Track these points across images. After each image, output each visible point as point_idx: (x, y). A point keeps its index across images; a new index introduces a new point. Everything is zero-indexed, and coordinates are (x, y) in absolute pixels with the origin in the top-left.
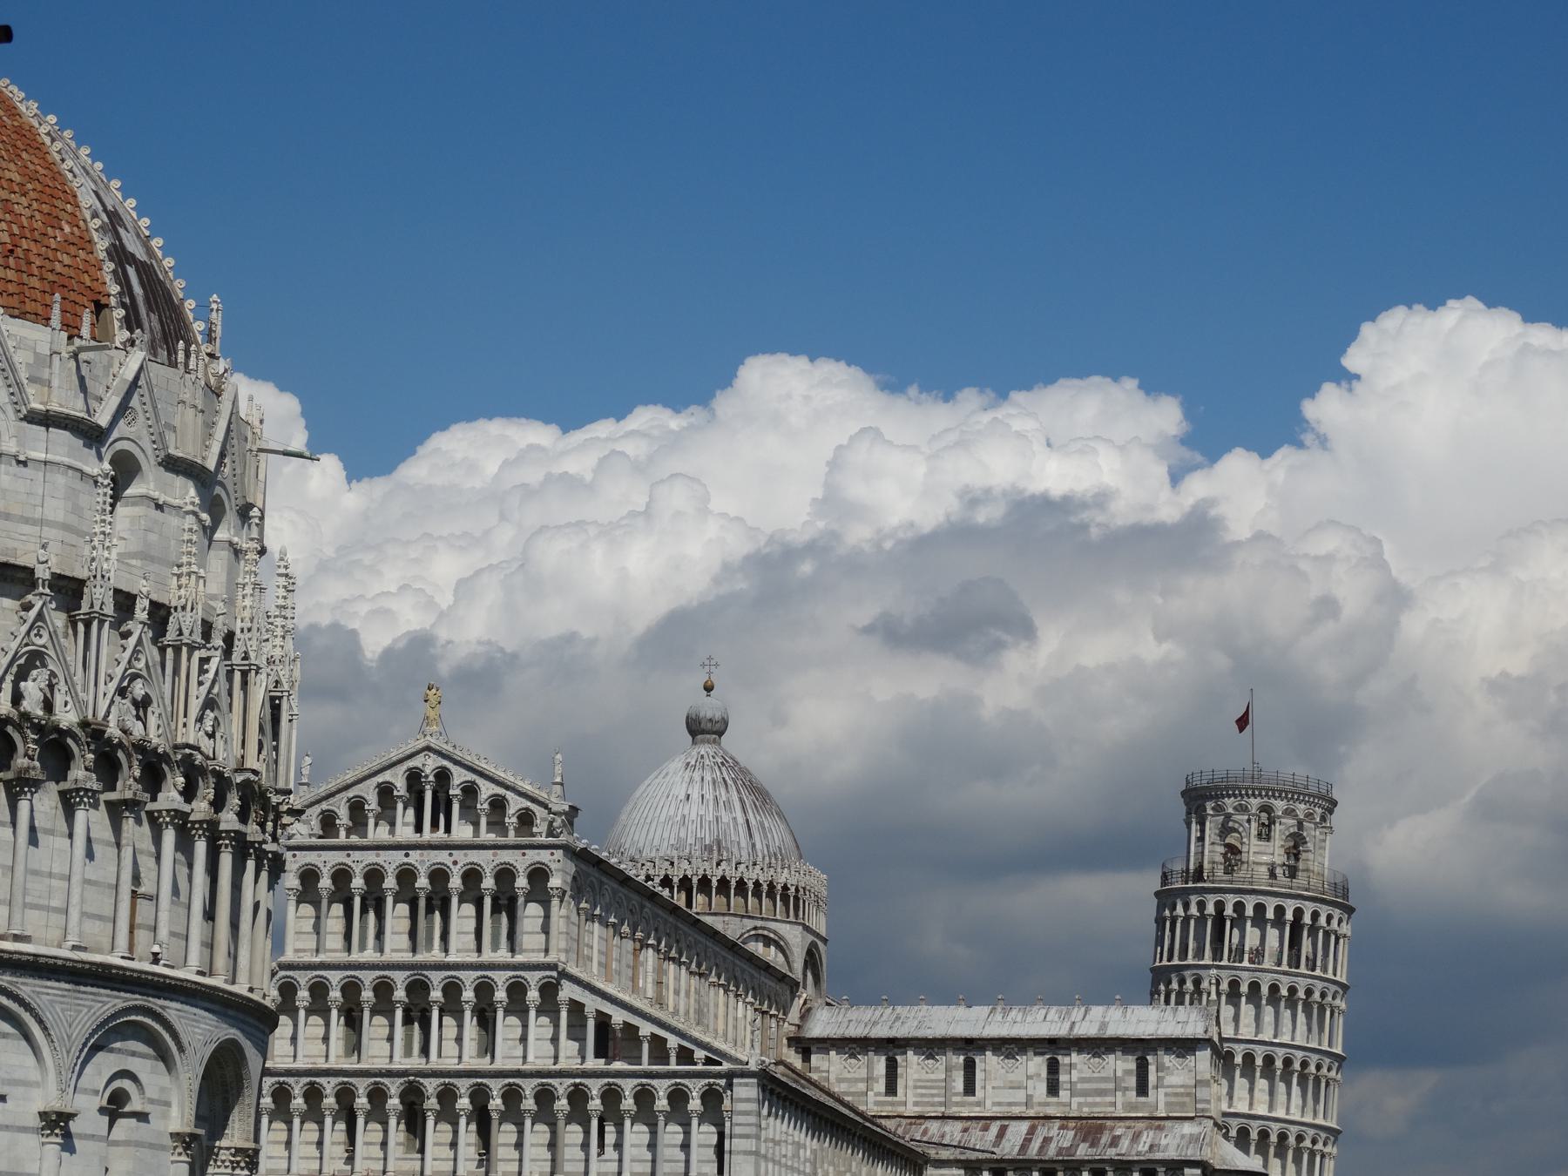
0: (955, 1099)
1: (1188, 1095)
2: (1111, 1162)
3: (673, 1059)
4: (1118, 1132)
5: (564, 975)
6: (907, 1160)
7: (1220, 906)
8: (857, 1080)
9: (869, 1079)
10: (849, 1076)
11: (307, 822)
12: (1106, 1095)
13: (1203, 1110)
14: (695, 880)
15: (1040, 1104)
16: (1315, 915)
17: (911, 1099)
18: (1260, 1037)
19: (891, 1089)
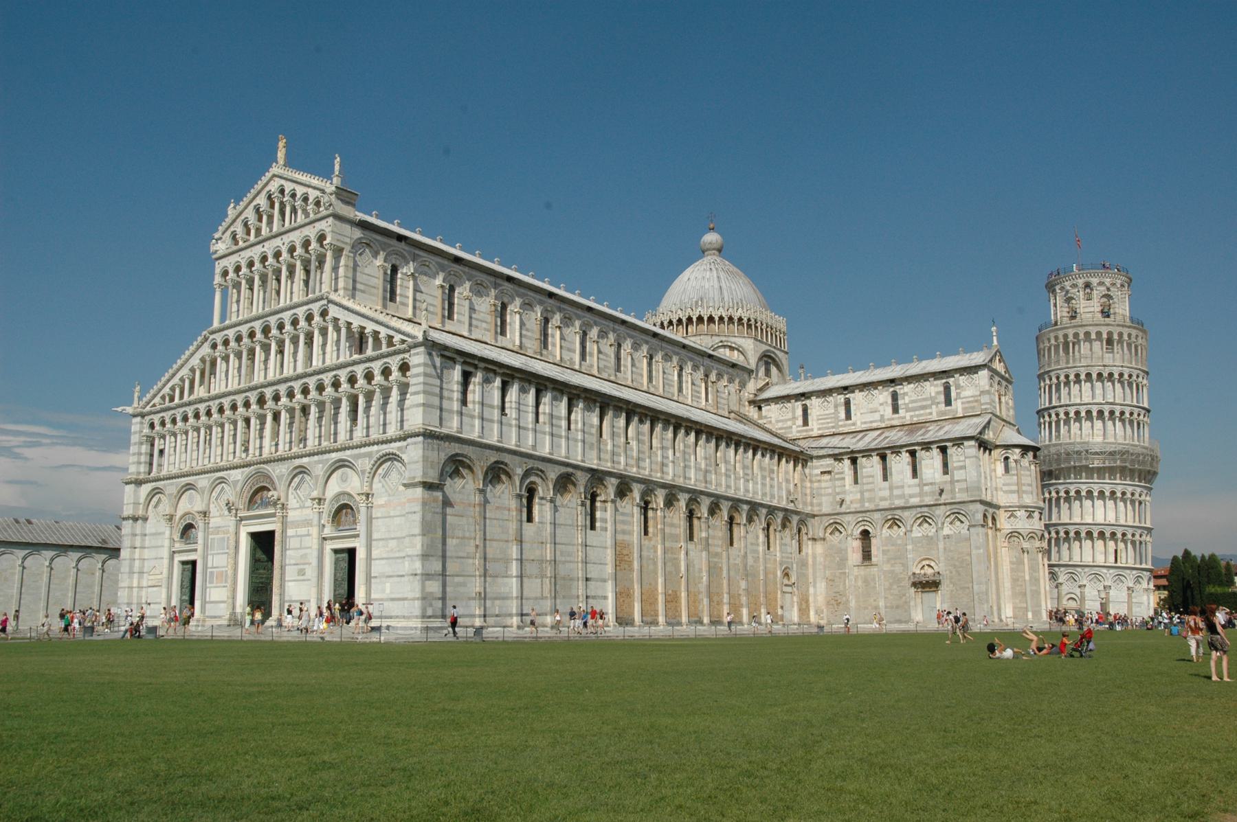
0: (840, 423)
1: (976, 401)
2: (918, 444)
3: (384, 346)
5: (330, 302)
7: (1066, 336)
8: (787, 420)
9: (794, 418)
10: (782, 418)
11: (224, 242)
13: (986, 409)
14: (684, 320)
15: (889, 420)
16: (1121, 334)
18: (1095, 401)
19: (806, 423)
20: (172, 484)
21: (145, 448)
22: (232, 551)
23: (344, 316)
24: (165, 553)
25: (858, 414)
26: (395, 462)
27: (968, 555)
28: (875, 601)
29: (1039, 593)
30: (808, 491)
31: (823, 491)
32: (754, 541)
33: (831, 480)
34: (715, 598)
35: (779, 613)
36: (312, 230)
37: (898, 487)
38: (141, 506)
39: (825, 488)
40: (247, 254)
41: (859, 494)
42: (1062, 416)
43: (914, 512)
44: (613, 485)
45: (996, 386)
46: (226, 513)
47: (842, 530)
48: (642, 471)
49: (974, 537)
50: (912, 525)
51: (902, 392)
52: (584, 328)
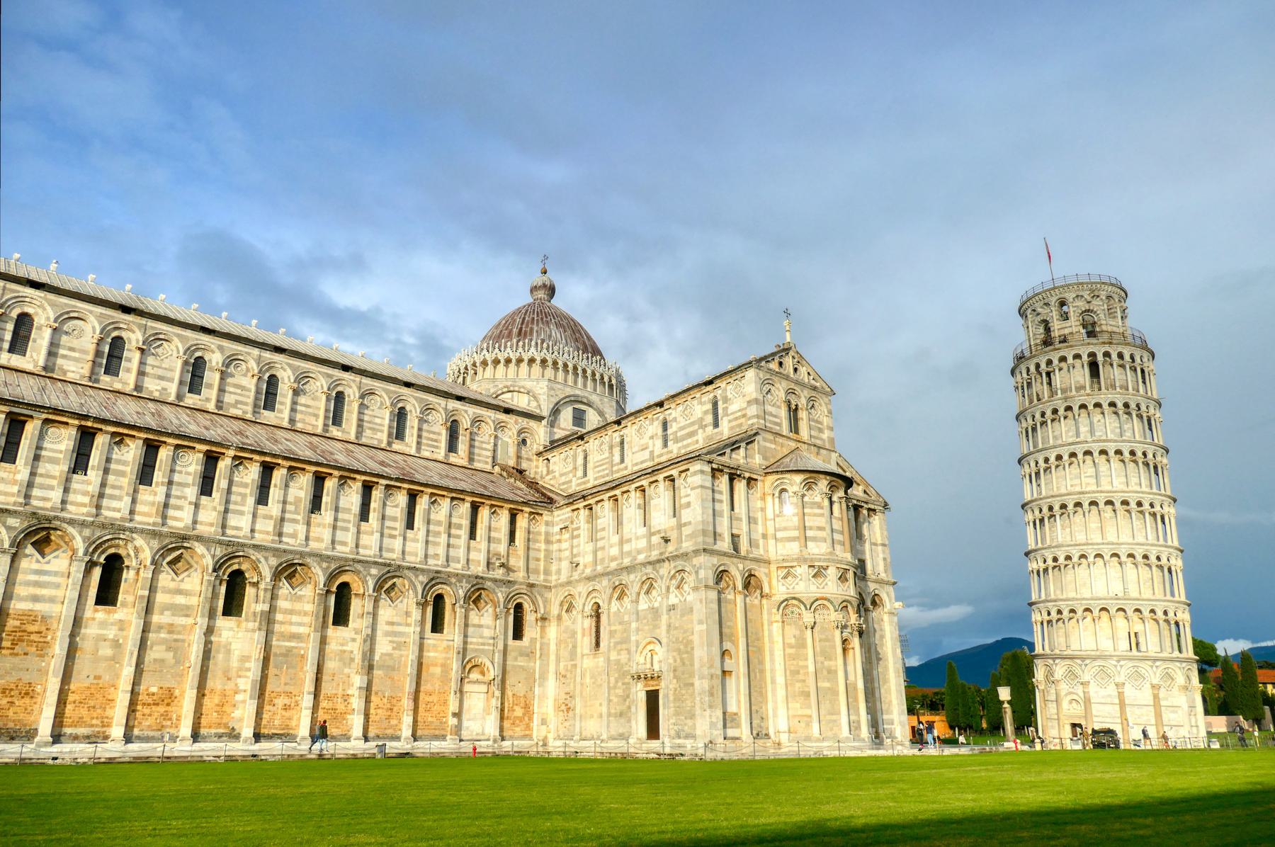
0: (615, 468)
1: (744, 416)
7: (1038, 366)
9: (575, 468)
10: (565, 471)
16: (1107, 354)
19: (585, 474)
25: (630, 454)
29: (836, 693)
32: (395, 620)
34: (280, 702)
35: (450, 723)
43: (640, 574)
50: (639, 594)
51: (671, 418)
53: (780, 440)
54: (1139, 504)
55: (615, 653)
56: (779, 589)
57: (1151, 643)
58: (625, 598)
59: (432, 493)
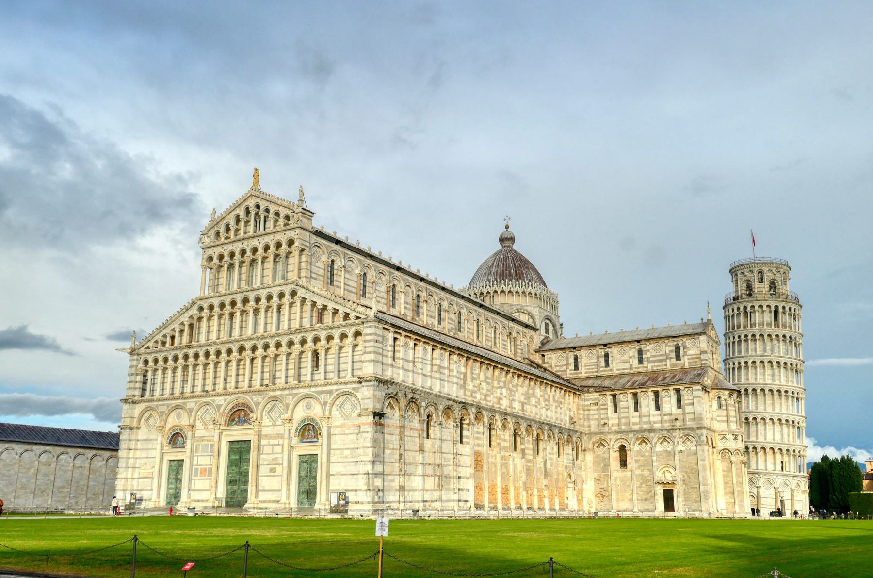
0: (601, 369)
1: (698, 358)
3: (342, 319)
4: (667, 376)
6: (565, 391)
7: (745, 308)
8: (563, 366)
9: (567, 365)
10: (558, 364)
12: (662, 362)
13: (705, 364)
15: (636, 368)
16: (784, 307)
17: (584, 371)
19: (576, 368)
20: (164, 405)
21: (139, 378)
22: (216, 454)
23: (309, 297)
24: (157, 454)
26: (349, 397)
27: (696, 464)
28: (630, 495)
30: (581, 417)
31: (591, 417)
33: (598, 409)
34: (529, 492)
36: (283, 236)
37: (645, 416)
38: (135, 420)
39: (593, 415)
40: (230, 248)
41: (618, 420)
42: (743, 364)
44: (473, 413)
45: (711, 347)
46: (211, 426)
47: (606, 444)
48: (489, 404)
49: (700, 453)
50: (656, 443)
51: (645, 349)
52: (439, 302)
53: (712, 371)
54: (793, 393)
55: (640, 471)
56: (720, 444)
57: (791, 466)
58: (644, 444)
59: (556, 387)
